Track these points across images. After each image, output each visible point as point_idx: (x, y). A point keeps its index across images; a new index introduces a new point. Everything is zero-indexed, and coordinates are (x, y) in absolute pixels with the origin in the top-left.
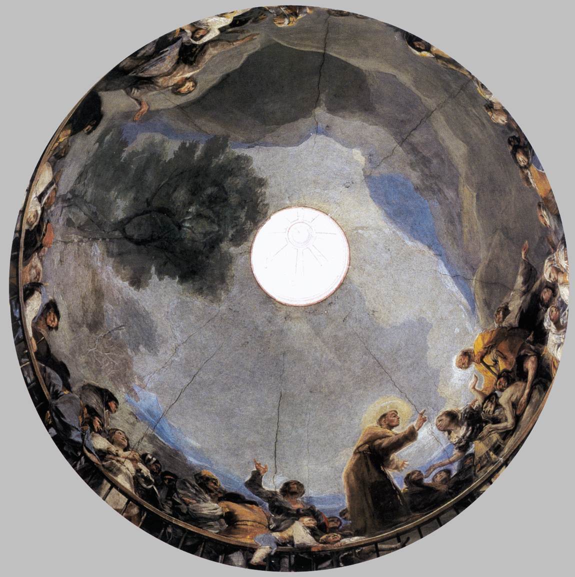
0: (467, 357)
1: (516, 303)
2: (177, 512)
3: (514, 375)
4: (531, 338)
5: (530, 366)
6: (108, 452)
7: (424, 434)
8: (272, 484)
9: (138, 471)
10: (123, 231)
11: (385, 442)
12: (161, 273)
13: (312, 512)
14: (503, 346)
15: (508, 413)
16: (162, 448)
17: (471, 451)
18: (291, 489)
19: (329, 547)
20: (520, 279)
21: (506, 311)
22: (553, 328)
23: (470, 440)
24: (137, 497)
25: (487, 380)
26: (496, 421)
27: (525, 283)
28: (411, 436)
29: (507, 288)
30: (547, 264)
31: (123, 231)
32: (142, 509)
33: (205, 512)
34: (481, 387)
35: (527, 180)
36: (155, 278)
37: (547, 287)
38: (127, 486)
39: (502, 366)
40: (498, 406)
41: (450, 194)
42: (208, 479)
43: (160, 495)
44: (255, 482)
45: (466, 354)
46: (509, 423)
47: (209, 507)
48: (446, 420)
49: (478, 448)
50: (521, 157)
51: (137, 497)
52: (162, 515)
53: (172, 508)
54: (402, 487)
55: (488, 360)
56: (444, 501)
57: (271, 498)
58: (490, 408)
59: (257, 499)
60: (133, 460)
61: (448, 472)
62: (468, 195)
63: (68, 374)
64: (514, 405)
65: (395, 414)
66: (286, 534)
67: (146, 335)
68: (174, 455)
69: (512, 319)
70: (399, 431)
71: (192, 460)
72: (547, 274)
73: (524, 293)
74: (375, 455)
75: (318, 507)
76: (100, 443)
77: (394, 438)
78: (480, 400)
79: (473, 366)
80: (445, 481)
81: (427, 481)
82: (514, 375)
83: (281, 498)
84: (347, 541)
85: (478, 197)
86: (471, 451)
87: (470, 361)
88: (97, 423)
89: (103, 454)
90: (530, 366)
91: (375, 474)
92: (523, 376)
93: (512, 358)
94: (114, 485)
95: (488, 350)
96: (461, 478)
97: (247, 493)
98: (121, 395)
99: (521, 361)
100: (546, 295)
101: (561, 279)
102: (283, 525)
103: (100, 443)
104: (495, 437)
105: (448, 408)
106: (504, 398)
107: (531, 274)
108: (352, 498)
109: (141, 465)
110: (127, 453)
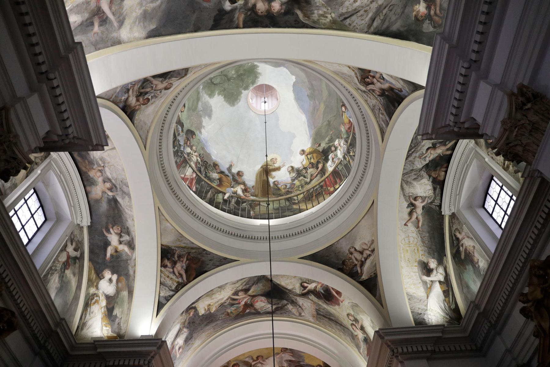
0: (303, 151)
1: (323, 145)
2: (206, 176)
3: (314, 166)
4: (324, 158)
5: (320, 166)
6: (190, 153)
7: (282, 169)
8: (234, 170)
9: (197, 160)
10: (211, 80)
11: (271, 168)
12: (219, 94)
13: (244, 184)
14: (315, 155)
15: (309, 176)
16: (206, 152)
17: (294, 182)
18: (240, 174)
19: (247, 198)
20: (327, 139)
21: (320, 145)
22: (331, 159)
23: (296, 178)
24: (195, 169)
25: (306, 163)
26: (305, 177)
27: (328, 141)
28: (278, 169)
29: (323, 138)
30: (337, 141)
31: (211, 80)
32: (197, 174)
33: (214, 177)
34: (304, 163)
35: (342, 115)
36: (216, 95)
37: (334, 147)
38: (193, 166)
39: (312, 161)
40: (307, 172)
41: (317, 103)
42: (217, 165)
43: (202, 169)
44: (229, 169)
45: (303, 151)
46: (308, 180)
47: (215, 175)
48: (290, 169)
49: (297, 182)
50: (343, 109)
51: (195, 169)
52: (203, 178)
53: (205, 174)
54: (272, 185)
55: (309, 156)
56: (282, 195)
57: (233, 176)
58: (304, 171)
59: (229, 175)
60: (196, 156)
61: (286, 186)
62: (322, 107)
63: (183, 126)
64: (312, 175)
65: (276, 159)
66: (235, 189)
67: (208, 112)
68: (209, 155)
69: (321, 149)
70: (277, 165)
71: (213, 157)
72: (336, 143)
73: (327, 143)
74: (266, 171)
75: (246, 183)
76: (188, 150)
77: (273, 167)
78: (302, 168)
79: (304, 155)
80: (284, 189)
81: (279, 186)
82: (314, 166)
83: (236, 176)
84: (252, 198)
85: (325, 109)
86: (294, 182)
87: (303, 154)
88: (188, 144)
89: (189, 154)
90: (320, 166)
91: (265, 178)
92: (317, 168)
93: (316, 160)
94: (190, 166)
95: (310, 153)
96: (290, 190)
97: (227, 172)
98: (197, 133)
99: (318, 162)
100: (333, 149)
101: (339, 147)
102: (235, 186)
103: (188, 150)
104: (303, 182)
105: (292, 165)
106: (310, 171)
107: (332, 140)
108: (256, 182)
109: (198, 158)
110: (196, 154)
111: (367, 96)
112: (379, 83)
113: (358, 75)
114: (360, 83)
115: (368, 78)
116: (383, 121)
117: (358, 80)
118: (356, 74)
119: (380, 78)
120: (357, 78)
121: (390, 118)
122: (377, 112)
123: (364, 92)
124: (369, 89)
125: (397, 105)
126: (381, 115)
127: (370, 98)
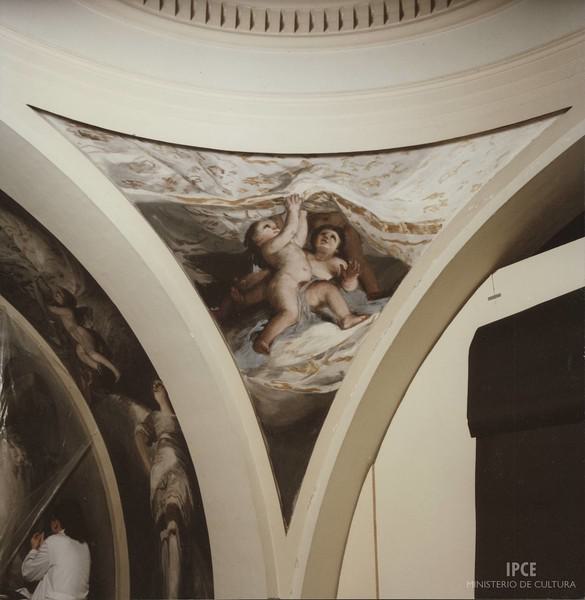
111: (267, 179)
112: (305, 276)
113: (370, 230)
114: (331, 196)
115: (341, 253)
116: (139, 167)
117: (342, 201)
118: (376, 224)
119: (326, 303)
120: (358, 210)
121: (148, 210)
122: (187, 163)
123: (286, 179)
124: (295, 208)
125: (203, 279)
126: (166, 172)
127: (252, 181)
